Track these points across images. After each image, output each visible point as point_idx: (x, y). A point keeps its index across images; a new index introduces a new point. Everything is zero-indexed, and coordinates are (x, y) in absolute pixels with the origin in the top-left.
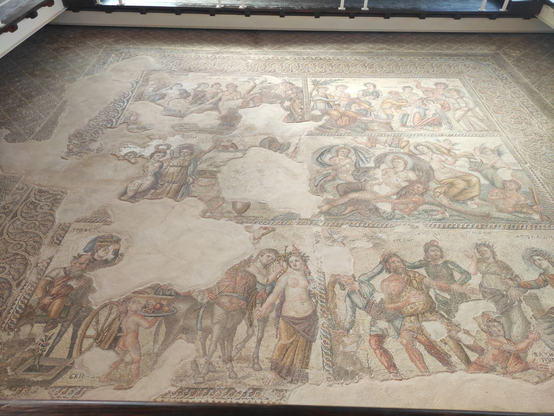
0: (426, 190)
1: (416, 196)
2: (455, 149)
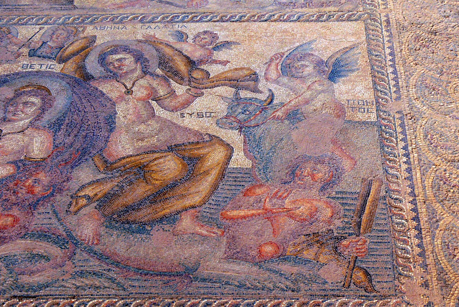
0: (56, 189)
1: (16, 212)
2: (215, 62)
